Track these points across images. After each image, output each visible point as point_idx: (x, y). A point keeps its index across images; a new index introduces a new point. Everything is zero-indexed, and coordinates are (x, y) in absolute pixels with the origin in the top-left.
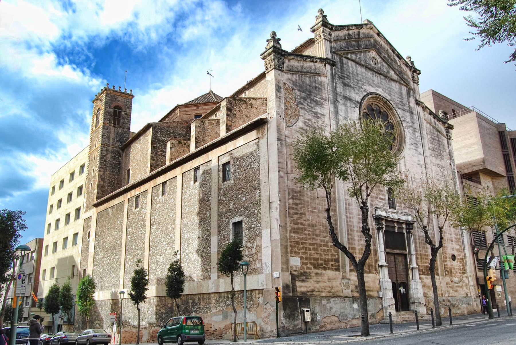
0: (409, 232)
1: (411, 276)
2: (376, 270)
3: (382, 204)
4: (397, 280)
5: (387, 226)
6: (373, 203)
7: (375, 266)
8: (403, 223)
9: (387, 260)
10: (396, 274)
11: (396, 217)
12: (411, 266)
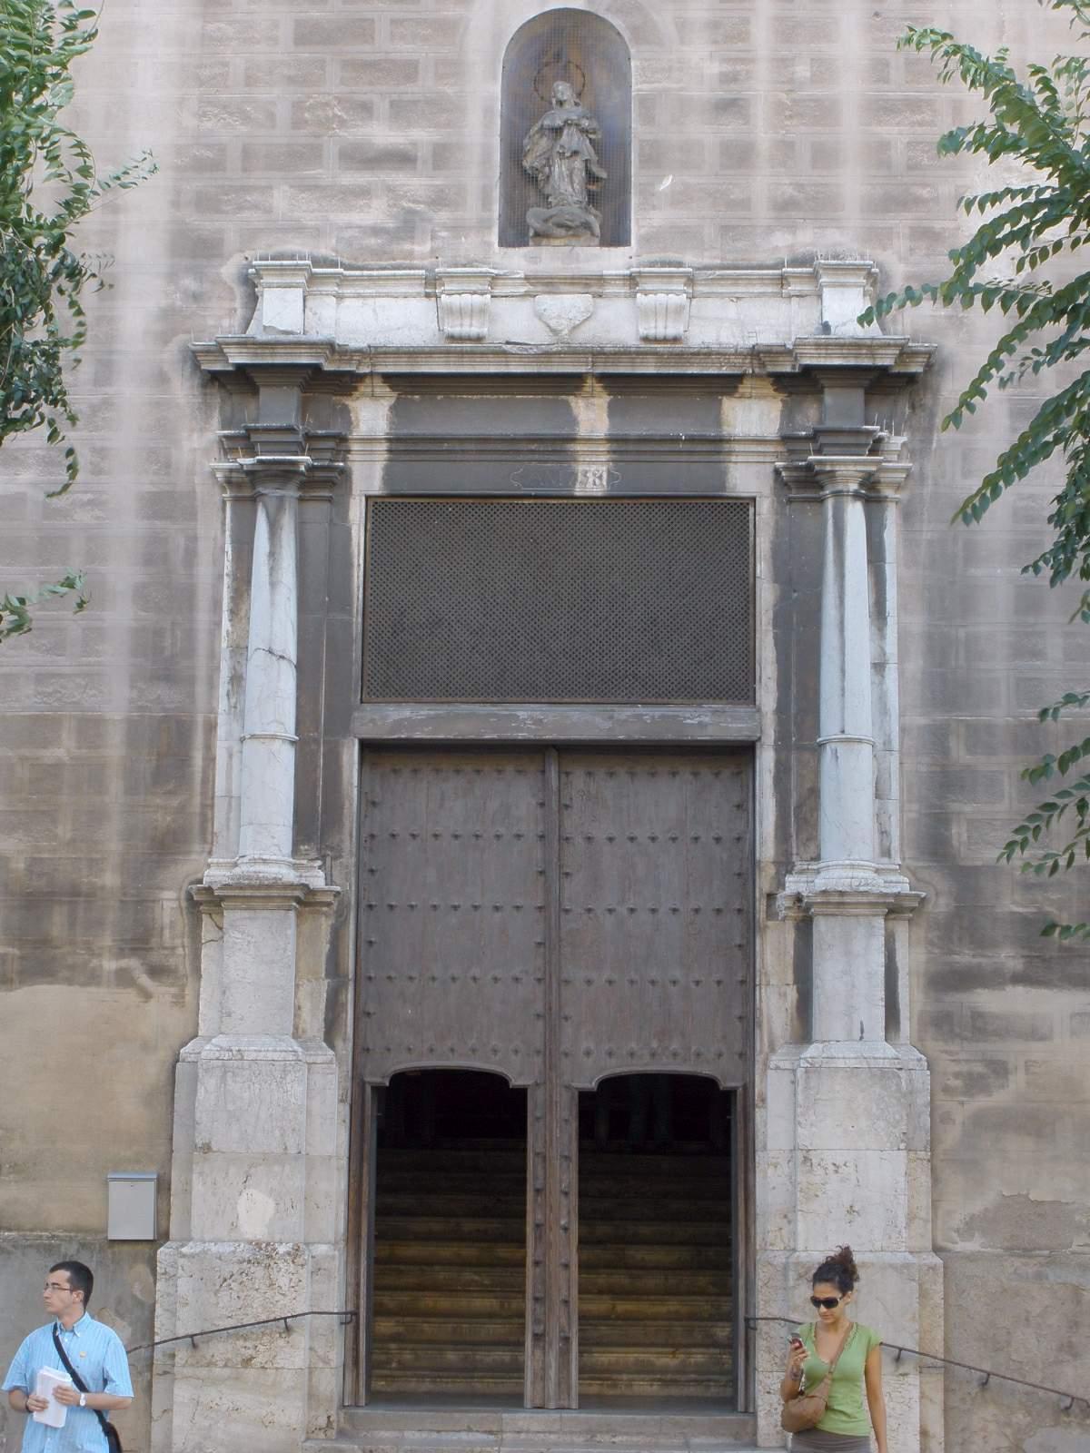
0: (803, 485)
1: (775, 1004)
2: (139, 941)
3: (376, 213)
4: (550, 1053)
5: (401, 446)
6: (229, 226)
7: (139, 903)
8: (728, 384)
9: (313, 824)
10: (550, 979)
11: (618, 324)
12: (793, 884)
